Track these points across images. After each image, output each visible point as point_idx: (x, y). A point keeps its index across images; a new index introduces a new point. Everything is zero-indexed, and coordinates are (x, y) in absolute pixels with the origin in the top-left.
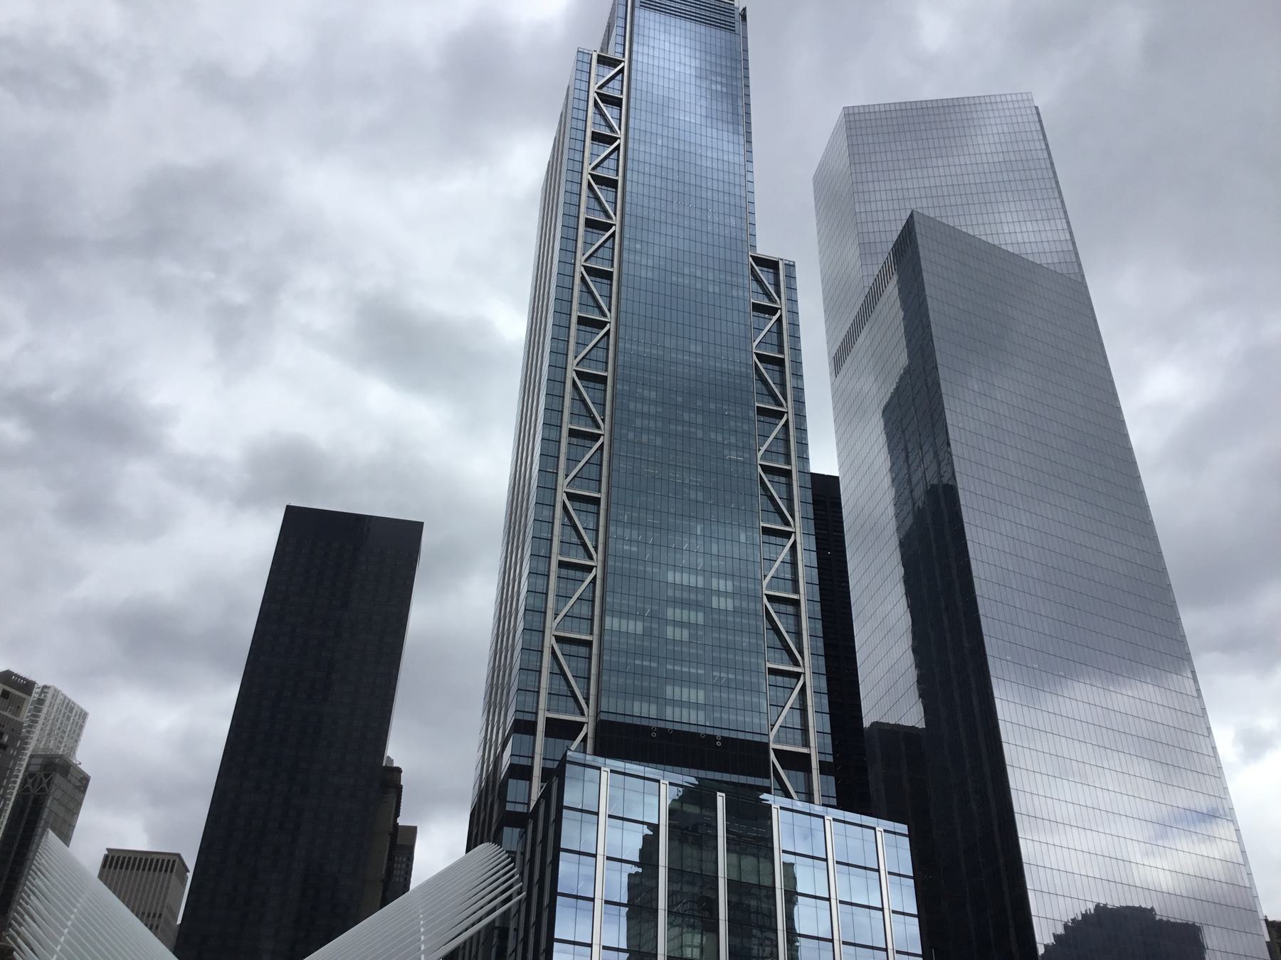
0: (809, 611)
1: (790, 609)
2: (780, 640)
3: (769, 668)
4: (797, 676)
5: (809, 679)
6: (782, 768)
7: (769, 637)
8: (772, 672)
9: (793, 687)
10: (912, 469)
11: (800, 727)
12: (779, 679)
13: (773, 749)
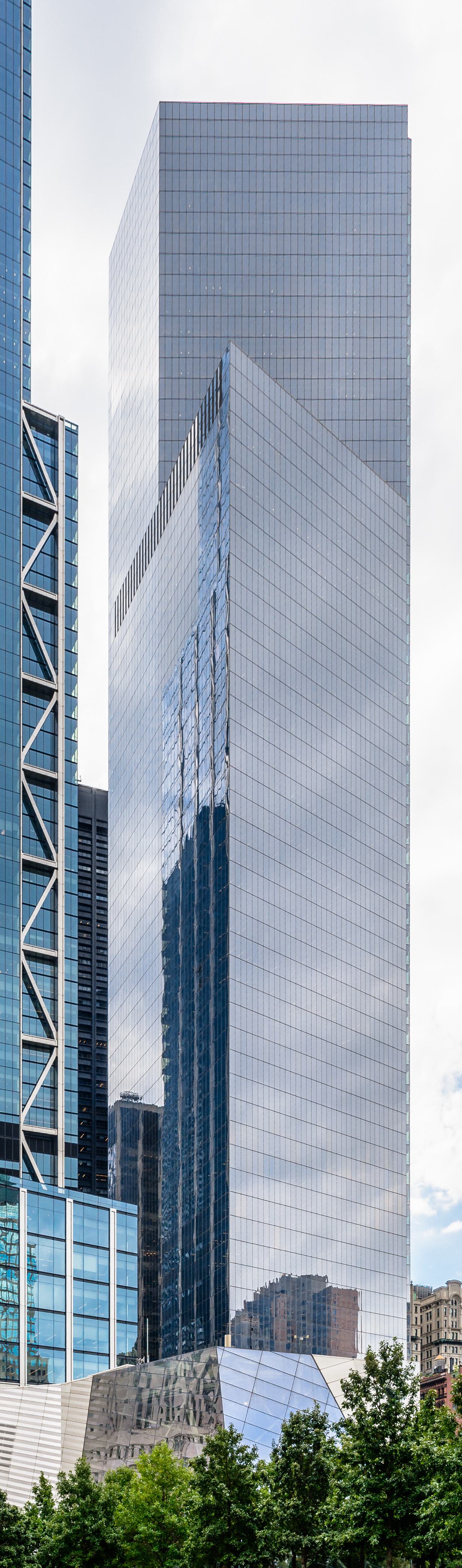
0: (67, 994)
1: (47, 969)
2: (36, 1008)
3: (23, 1040)
4: (50, 1049)
5: (60, 1053)
6: (31, 1151)
7: (26, 1004)
8: (27, 1045)
9: (46, 1063)
10: (186, 783)
11: (49, 1107)
12: (33, 1053)
13: (25, 1132)
